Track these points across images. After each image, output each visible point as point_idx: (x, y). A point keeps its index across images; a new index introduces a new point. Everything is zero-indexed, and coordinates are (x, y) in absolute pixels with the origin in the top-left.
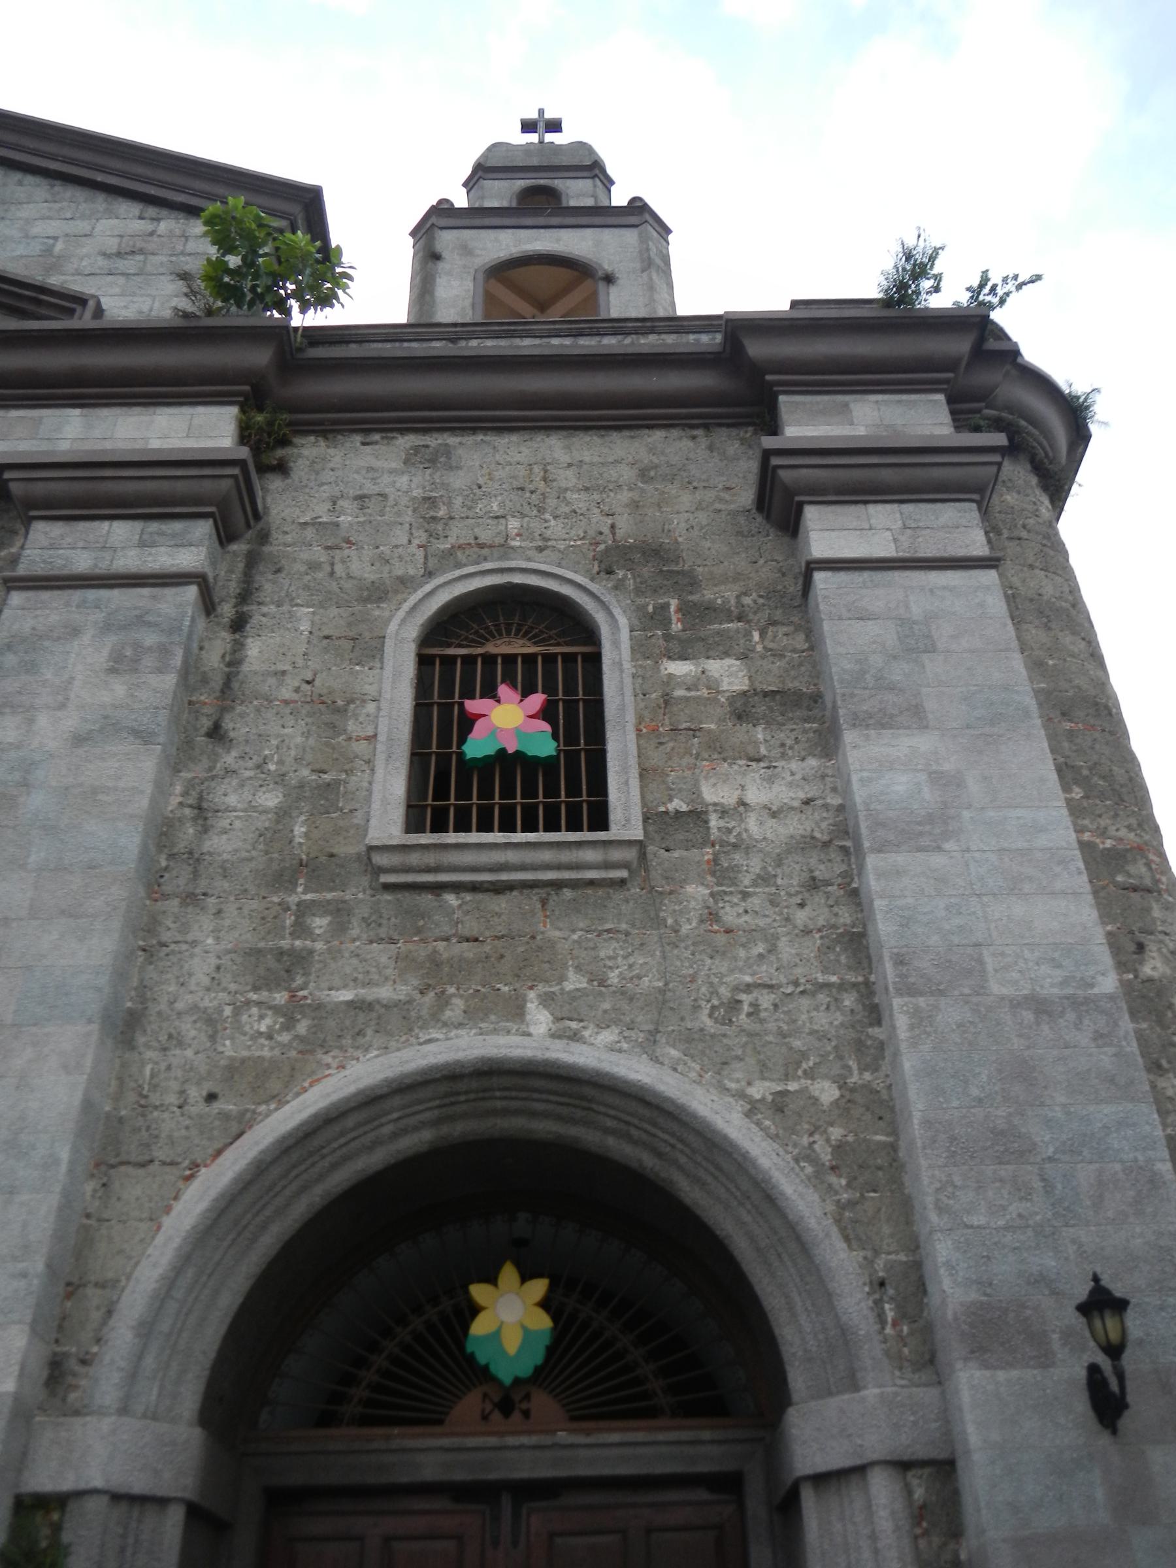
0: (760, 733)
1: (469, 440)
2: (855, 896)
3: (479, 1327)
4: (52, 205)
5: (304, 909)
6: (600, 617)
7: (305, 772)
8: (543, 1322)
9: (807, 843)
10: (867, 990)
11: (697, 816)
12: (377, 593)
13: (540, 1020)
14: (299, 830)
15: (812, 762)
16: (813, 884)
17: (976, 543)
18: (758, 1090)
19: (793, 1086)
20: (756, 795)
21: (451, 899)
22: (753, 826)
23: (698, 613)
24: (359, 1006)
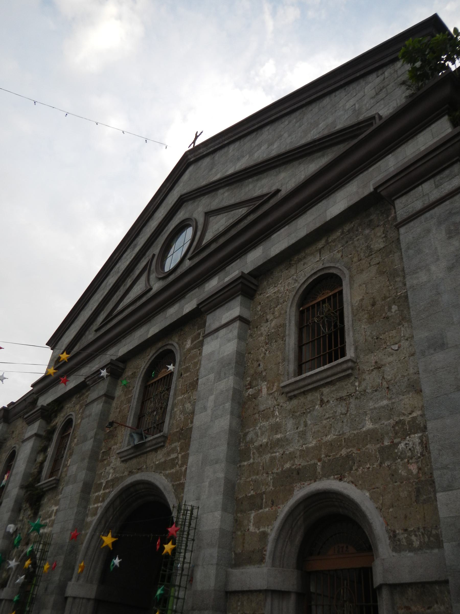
4: (348, 95)
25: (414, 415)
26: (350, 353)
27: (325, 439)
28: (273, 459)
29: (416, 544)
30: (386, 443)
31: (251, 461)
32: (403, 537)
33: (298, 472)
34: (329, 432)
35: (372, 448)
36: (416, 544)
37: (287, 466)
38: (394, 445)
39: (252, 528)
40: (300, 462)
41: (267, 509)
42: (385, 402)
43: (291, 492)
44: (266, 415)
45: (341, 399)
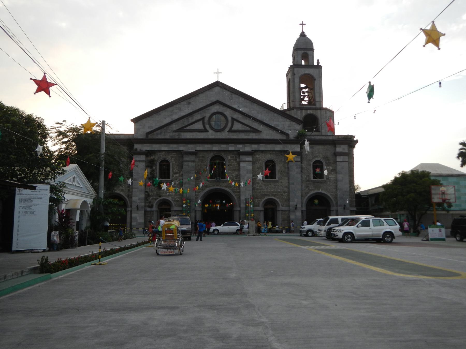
0: (333, 172)
1: (315, 146)
2: (337, 183)
3: (315, 202)
5: (308, 183)
6: (324, 163)
7: (307, 174)
8: (318, 202)
9: (334, 180)
10: (337, 189)
11: (329, 178)
12: (310, 160)
13: (320, 190)
14: (307, 178)
15: (335, 175)
16: (334, 182)
17: (347, 160)
18: (331, 194)
19: (333, 194)
20: (332, 177)
21: (316, 183)
22: (332, 179)
23: (330, 163)
24: (312, 189)
25: (286, 191)
26: (277, 179)
27: (272, 191)
28: (260, 192)
29: (285, 206)
30: (282, 194)
31: (255, 191)
32: (283, 205)
33: (266, 194)
34: (272, 190)
35: (280, 194)
36: (285, 206)
37: (264, 193)
38: (283, 194)
39: (256, 201)
40: (267, 193)
41: (260, 199)
42: (282, 188)
43: (265, 197)
44: (258, 183)
45: (275, 185)
